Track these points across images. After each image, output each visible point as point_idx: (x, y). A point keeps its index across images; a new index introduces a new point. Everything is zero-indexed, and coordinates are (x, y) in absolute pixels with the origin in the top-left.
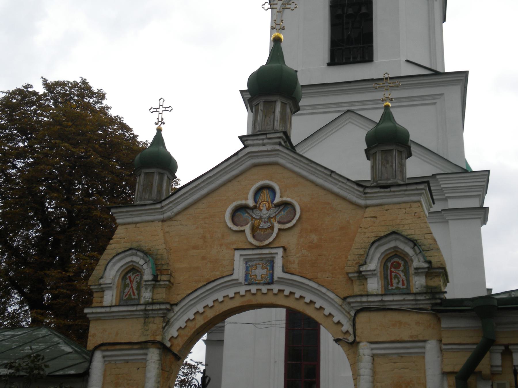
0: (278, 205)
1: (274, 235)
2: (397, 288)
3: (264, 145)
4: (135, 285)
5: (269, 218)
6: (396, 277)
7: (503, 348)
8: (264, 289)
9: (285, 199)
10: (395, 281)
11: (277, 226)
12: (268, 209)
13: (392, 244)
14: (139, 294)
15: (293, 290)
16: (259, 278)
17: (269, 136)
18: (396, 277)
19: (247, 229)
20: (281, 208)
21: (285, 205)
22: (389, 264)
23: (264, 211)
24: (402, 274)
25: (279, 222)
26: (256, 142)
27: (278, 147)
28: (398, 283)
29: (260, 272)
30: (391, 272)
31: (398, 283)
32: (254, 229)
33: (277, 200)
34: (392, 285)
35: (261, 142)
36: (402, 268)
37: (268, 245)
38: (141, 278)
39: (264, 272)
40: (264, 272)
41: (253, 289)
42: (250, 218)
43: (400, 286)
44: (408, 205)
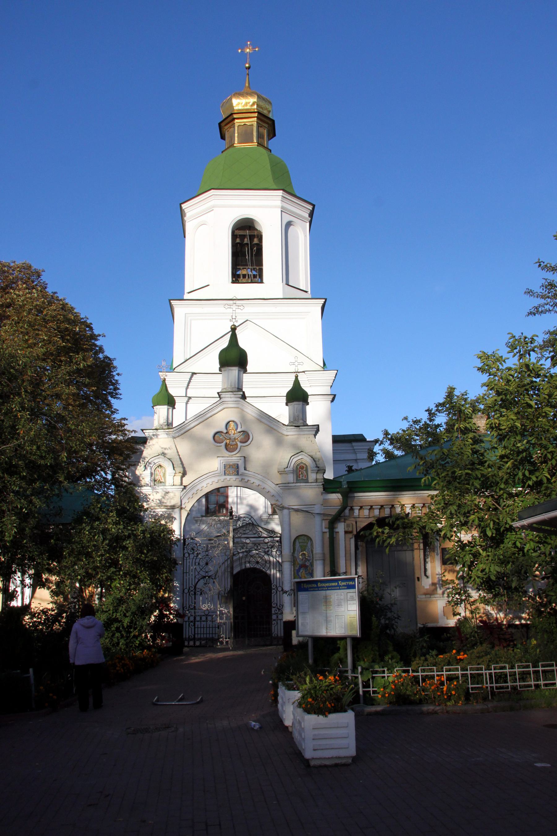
2: (302, 479)
4: (162, 474)
5: (235, 439)
7: (350, 508)
13: (300, 457)
14: (165, 480)
20: (241, 433)
22: (298, 467)
24: (305, 472)
25: (241, 442)
27: (239, 399)
28: (303, 476)
30: (300, 471)
31: (303, 476)
32: (226, 445)
34: (300, 477)
35: (229, 396)
36: (305, 469)
38: (165, 471)
43: (304, 478)
44: (308, 436)
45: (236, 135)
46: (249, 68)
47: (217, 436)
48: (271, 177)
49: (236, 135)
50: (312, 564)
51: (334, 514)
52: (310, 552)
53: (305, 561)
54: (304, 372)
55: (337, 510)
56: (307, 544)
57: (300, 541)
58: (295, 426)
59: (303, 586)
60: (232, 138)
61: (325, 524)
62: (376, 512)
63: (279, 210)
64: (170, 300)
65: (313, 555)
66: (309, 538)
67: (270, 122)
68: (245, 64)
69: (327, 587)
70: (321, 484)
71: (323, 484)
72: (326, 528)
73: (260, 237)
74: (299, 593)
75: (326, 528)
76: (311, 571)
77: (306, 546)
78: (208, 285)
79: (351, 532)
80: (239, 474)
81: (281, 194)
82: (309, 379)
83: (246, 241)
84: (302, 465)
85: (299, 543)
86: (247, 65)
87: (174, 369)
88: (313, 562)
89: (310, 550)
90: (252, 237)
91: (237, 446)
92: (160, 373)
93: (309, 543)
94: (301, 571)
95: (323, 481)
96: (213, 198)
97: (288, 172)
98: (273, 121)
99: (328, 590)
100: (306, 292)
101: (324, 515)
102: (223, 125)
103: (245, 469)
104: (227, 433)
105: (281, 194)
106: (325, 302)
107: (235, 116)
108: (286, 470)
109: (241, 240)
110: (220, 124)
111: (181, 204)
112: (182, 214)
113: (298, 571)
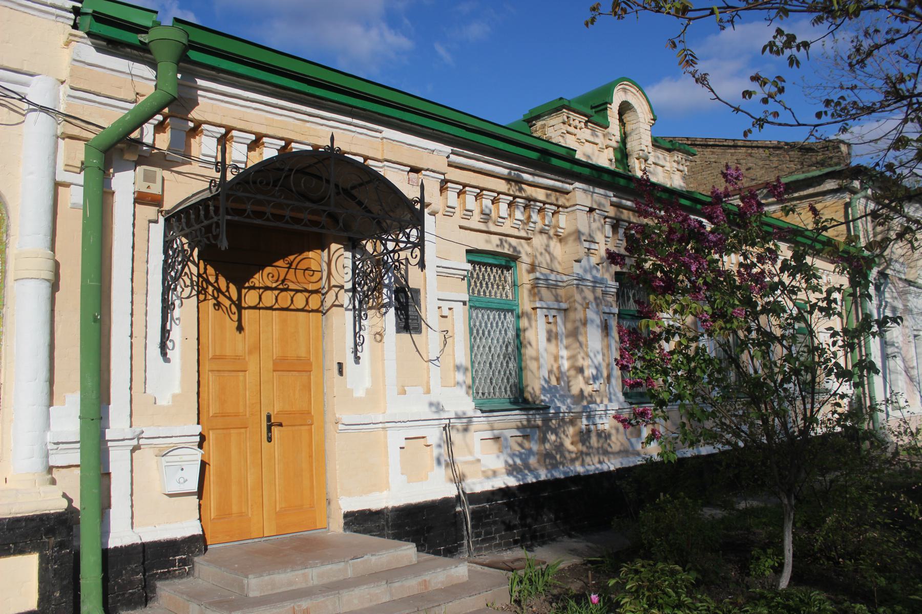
55: (120, 114)
72: (68, 168)
75: (68, 168)
79: (156, 201)
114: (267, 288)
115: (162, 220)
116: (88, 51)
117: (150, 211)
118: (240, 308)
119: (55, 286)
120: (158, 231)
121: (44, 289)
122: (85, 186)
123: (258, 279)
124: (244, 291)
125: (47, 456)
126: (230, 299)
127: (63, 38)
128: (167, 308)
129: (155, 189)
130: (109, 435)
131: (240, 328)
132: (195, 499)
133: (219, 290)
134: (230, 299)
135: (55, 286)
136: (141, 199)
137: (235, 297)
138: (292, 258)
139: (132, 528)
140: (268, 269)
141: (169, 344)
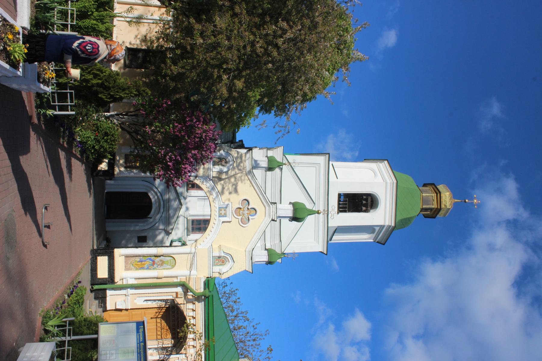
0: (248, 218)
1: (236, 217)
2: (215, 262)
3: (272, 212)
5: (244, 214)
6: (219, 261)
8: (217, 214)
9: (250, 220)
10: (217, 261)
11: (240, 217)
12: (247, 213)
15: (216, 225)
16: (221, 212)
17: (276, 215)
18: (219, 261)
19: (241, 206)
21: (249, 220)
23: (247, 212)
25: (242, 218)
26: (274, 209)
27: (271, 218)
29: (223, 212)
30: (221, 260)
33: (250, 217)
35: (274, 211)
36: (222, 264)
37: (233, 215)
39: (223, 214)
40: (223, 214)
41: (217, 210)
42: (244, 206)
45: (427, 195)
46: (465, 202)
47: (246, 201)
48: (403, 218)
49: (427, 195)
50: (154, 269)
51: (190, 285)
52: (163, 268)
53: (157, 264)
54: (281, 241)
55: (193, 288)
56: (169, 265)
57: (172, 260)
58: (252, 257)
59: (141, 328)
60: (426, 192)
61: (183, 279)
62: (191, 314)
63: (382, 224)
64: (329, 154)
65: (161, 269)
66: (173, 267)
67: (434, 215)
68: (467, 199)
69: (140, 352)
70: (212, 276)
71: (211, 277)
72: (180, 279)
73: (366, 211)
74: (135, 323)
75: (180, 279)
76: (150, 268)
77: (168, 264)
78: (337, 178)
79: (177, 297)
80: (220, 218)
81: (392, 225)
82: (276, 244)
83: (364, 202)
84: (225, 262)
85: (170, 260)
86: (467, 201)
87: (285, 156)
88: (157, 269)
89: (165, 268)
90: (366, 207)
91: (239, 216)
92: (283, 147)
93: (170, 267)
94: (150, 261)
95: (214, 276)
96: (391, 181)
97: (405, 227)
98: (435, 218)
99: (138, 353)
100: (331, 240)
101: (190, 278)
102: (433, 186)
103: (223, 222)
104: (248, 209)
105: (392, 225)
106: (325, 254)
107: (439, 195)
108: (222, 251)
109: (365, 199)
110: (433, 184)
111: (387, 160)
112: (382, 160)
113: (150, 259)
114: (161, 324)
115: (174, 298)
116: (203, 280)
117: (175, 295)
118: (156, 318)
119: (157, 278)
120: (171, 298)
121: (156, 276)
122: (177, 282)
123: (163, 321)
124: (160, 319)
125: (125, 278)
126: (158, 315)
127: (205, 275)
128: (155, 300)
129: (179, 296)
130: (129, 289)
131: (152, 318)
132: (114, 308)
133: (160, 313)
134: (158, 315)
135: (157, 278)
136: (177, 293)
137: (159, 316)
138: (169, 330)
139: (110, 295)
140: (166, 324)
141: (147, 302)
